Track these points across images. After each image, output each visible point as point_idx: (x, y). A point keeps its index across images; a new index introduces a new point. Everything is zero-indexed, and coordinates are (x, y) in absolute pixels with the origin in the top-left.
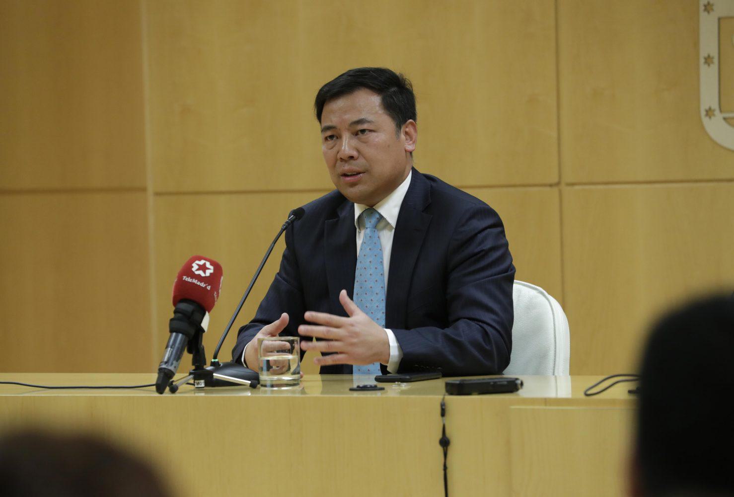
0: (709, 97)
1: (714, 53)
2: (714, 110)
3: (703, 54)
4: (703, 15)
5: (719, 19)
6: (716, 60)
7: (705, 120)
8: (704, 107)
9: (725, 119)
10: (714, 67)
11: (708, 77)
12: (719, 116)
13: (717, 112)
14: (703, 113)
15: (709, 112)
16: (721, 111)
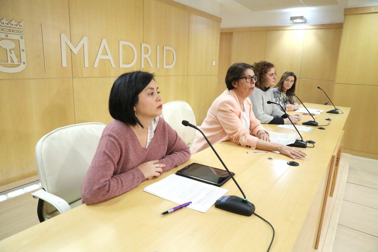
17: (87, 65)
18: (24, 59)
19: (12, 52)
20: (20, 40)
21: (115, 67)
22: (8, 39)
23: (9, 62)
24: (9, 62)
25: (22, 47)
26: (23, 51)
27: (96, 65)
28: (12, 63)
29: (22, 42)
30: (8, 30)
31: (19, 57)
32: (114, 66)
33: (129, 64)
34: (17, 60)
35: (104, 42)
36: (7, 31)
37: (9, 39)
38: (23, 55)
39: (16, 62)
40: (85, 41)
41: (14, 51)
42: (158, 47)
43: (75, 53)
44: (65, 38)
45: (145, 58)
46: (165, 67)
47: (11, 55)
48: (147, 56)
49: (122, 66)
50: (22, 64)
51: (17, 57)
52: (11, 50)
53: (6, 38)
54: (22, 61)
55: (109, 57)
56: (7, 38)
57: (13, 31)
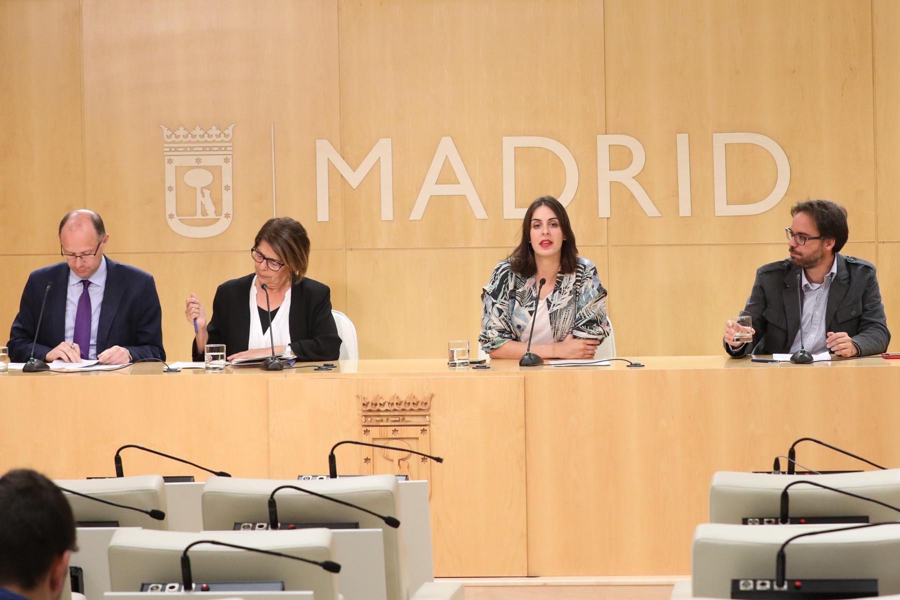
0: (171, 208)
1: (173, 185)
2: (174, 215)
3: (167, 185)
4: (167, 165)
5: (176, 167)
7: (169, 220)
8: (168, 213)
9: (179, 219)
10: (174, 192)
12: (176, 218)
13: (175, 216)
14: (168, 216)
15: (171, 216)
16: (178, 216)
17: (387, 212)
18: (227, 207)
19: (207, 192)
20: (224, 165)
21: (486, 217)
23: (199, 216)
24: (199, 216)
25: (227, 180)
26: (227, 188)
27: (417, 214)
28: (203, 216)
29: (227, 169)
30: (201, 149)
31: (217, 203)
32: (480, 212)
34: (214, 208)
35: (447, 148)
36: (201, 151)
38: (227, 197)
39: (212, 215)
40: (383, 150)
41: (209, 190)
42: (682, 140)
43: (354, 184)
44: (326, 151)
45: (615, 186)
46: (722, 208)
48: (625, 177)
50: (222, 218)
51: (214, 204)
52: (204, 190)
53: (197, 164)
54: (224, 212)
55: (465, 187)
56: (200, 164)
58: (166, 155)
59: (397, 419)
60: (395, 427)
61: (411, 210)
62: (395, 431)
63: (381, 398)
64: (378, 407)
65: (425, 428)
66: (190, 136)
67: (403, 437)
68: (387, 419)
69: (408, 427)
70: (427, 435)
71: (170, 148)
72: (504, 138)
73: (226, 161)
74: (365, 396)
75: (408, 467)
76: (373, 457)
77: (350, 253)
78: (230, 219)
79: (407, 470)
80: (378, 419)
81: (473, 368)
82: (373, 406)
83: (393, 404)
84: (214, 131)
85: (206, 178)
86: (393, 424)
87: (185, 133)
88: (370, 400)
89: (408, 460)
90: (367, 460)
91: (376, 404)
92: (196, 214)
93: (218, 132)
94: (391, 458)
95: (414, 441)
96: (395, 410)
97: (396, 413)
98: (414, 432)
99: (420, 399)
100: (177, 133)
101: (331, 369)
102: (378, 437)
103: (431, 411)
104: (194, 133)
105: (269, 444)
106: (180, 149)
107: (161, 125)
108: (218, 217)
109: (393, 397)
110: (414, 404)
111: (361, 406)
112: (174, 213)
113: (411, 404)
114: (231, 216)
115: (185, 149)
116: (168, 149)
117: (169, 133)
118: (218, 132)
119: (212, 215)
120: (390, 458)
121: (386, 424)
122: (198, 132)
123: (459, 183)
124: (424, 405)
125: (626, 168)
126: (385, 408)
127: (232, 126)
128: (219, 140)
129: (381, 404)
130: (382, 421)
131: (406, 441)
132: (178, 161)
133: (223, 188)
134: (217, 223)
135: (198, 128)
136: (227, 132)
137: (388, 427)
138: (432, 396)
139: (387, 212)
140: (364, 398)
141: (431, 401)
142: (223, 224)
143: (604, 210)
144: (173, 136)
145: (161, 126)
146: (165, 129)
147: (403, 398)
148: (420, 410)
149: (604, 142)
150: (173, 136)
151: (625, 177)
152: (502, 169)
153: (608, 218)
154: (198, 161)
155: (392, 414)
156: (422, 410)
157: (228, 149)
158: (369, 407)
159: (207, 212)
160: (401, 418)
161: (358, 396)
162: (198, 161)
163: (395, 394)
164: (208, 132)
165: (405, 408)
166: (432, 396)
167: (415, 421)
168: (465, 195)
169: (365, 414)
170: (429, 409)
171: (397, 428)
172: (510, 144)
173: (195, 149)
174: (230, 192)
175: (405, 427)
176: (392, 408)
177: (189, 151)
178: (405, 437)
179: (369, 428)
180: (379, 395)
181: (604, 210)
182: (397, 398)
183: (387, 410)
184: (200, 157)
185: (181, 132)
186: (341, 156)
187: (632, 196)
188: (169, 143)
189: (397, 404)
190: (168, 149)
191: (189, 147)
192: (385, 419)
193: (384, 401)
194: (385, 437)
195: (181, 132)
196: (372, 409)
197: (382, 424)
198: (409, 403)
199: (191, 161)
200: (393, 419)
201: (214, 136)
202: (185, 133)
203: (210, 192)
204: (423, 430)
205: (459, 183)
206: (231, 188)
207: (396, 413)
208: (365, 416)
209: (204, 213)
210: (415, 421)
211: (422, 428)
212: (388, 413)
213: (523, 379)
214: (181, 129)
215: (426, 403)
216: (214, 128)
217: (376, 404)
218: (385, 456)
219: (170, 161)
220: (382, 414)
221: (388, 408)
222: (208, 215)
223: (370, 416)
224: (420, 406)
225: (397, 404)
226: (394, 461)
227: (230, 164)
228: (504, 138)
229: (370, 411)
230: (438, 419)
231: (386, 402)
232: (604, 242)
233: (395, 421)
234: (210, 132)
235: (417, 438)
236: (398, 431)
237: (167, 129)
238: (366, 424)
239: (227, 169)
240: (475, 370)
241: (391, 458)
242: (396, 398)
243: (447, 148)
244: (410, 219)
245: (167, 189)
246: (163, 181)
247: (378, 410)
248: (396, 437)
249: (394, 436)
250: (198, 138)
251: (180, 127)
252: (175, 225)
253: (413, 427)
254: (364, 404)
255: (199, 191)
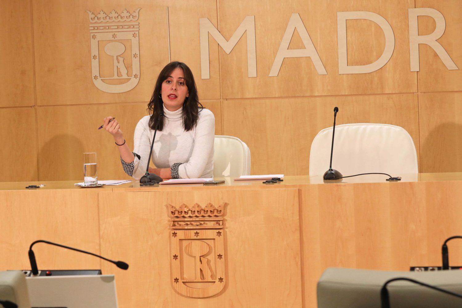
0: (95, 72)
1: (97, 55)
2: (98, 76)
3: (93, 54)
4: (92, 40)
6: (98, 57)
7: (94, 80)
8: (93, 75)
10: (97, 60)
11: (95, 63)
12: (99, 79)
13: (99, 77)
14: (93, 78)
15: (96, 77)
17: (252, 72)
18: (135, 70)
19: (121, 59)
22: (116, 41)
23: (116, 77)
25: (135, 50)
26: (135, 56)
27: (274, 72)
29: (135, 41)
30: (117, 27)
31: (128, 67)
32: (321, 70)
33: (369, 62)
37: (119, 41)
38: (135, 62)
39: (125, 76)
43: (228, 51)
47: (117, 64)
48: (431, 40)
49: (344, 69)
50: (133, 79)
52: (119, 58)
55: (309, 51)
56: (116, 39)
57: (123, 27)
58: (91, 33)
59: (198, 224)
60: (197, 231)
61: (269, 69)
62: (197, 233)
63: (186, 207)
64: (183, 214)
65: (220, 231)
66: (108, 17)
67: (203, 238)
68: (190, 224)
69: (207, 230)
70: (222, 237)
71: (94, 27)
72: (338, 13)
73: (134, 35)
74: (173, 205)
75: (208, 262)
76: (180, 255)
77: (226, 102)
78: (138, 79)
79: (207, 265)
80: (183, 223)
81: (263, 183)
82: (180, 213)
83: (194, 211)
84: (125, 14)
85: (121, 49)
86: (195, 228)
87: (104, 16)
88: (178, 208)
89: (209, 257)
90: (175, 257)
91: (182, 212)
92: (114, 76)
93: (128, 14)
94: (194, 256)
95: (213, 240)
96: (196, 216)
97: (197, 219)
98: (212, 234)
99: (216, 207)
100: (99, 16)
101: (154, 185)
102: (183, 238)
103: (225, 218)
104: (110, 15)
105: (100, 245)
106: (102, 28)
107: (88, 10)
108: (129, 78)
109: (195, 205)
110: (211, 211)
111: (170, 213)
112: (98, 75)
113: (209, 212)
114: (139, 76)
115: (105, 27)
116: (92, 28)
117: (93, 16)
118: (128, 14)
119: (125, 76)
120: (193, 255)
121: (189, 228)
122: (114, 15)
123: (305, 48)
124: (219, 212)
125: (430, 34)
126: (188, 215)
127: (139, 9)
128: (129, 20)
129: (185, 212)
130: (187, 225)
131: (204, 241)
132: (99, 37)
133: (133, 56)
134: (128, 83)
135: (113, 12)
136: (134, 14)
137: (191, 231)
138: (226, 205)
139: (252, 72)
140: (172, 207)
141: (224, 209)
142: (134, 82)
143: (415, 66)
144: (96, 18)
145: (87, 11)
146: (90, 13)
147: (203, 206)
148: (216, 216)
149: (414, 13)
150: (96, 18)
151: (431, 40)
152: (337, 37)
153: (417, 72)
154: (114, 36)
155: (194, 219)
156: (218, 216)
157: (136, 27)
158: (176, 214)
159: (121, 74)
160: (202, 223)
161: (167, 206)
162: (114, 36)
163: (197, 203)
164: (121, 15)
165: (204, 215)
166: (226, 205)
167: (211, 225)
168: (309, 57)
169: (173, 220)
170: (223, 215)
171: (198, 231)
172: (342, 17)
173: (112, 27)
174: (138, 59)
175: (205, 230)
176: (194, 215)
177: (107, 29)
178: (205, 238)
179: (176, 231)
180: (184, 204)
181: (415, 66)
182: (198, 206)
183: (190, 217)
184: (116, 33)
185: (102, 15)
186: (218, 30)
187: (436, 55)
188: (94, 23)
189: (198, 211)
190: (92, 28)
191: (108, 26)
192: (189, 223)
193: (188, 209)
194: (189, 238)
195: (102, 15)
196: (179, 216)
197: (186, 228)
198: (207, 211)
199: (109, 36)
200: (194, 223)
201: (125, 17)
202: (104, 16)
203: (123, 59)
204: (219, 233)
205: (305, 48)
206: (138, 56)
207: (197, 219)
208: (174, 221)
209: (119, 74)
210: (211, 225)
211: (218, 231)
212: (191, 219)
213: (297, 190)
214: (102, 13)
215: (221, 211)
216: (125, 12)
217: (182, 212)
218: (190, 254)
219: (94, 37)
220: (186, 219)
221: (191, 215)
222: (122, 76)
223: (176, 221)
224: (216, 213)
225: (198, 211)
226: (196, 257)
227: (137, 38)
228: (339, 14)
229: (177, 217)
230: (231, 225)
231: (189, 210)
232: (415, 90)
233: (197, 225)
234: (122, 15)
235: (214, 239)
236: (199, 233)
237: (92, 13)
238: (174, 228)
239: (135, 41)
240: (265, 185)
241: (194, 255)
242: (196, 206)
243: (295, 22)
244: (270, 75)
245: (92, 57)
246: (90, 51)
247: (184, 217)
248: (197, 238)
249: (195, 238)
250: (114, 19)
251: (101, 11)
252: (98, 83)
253: (210, 230)
254: (172, 212)
255: (115, 58)
